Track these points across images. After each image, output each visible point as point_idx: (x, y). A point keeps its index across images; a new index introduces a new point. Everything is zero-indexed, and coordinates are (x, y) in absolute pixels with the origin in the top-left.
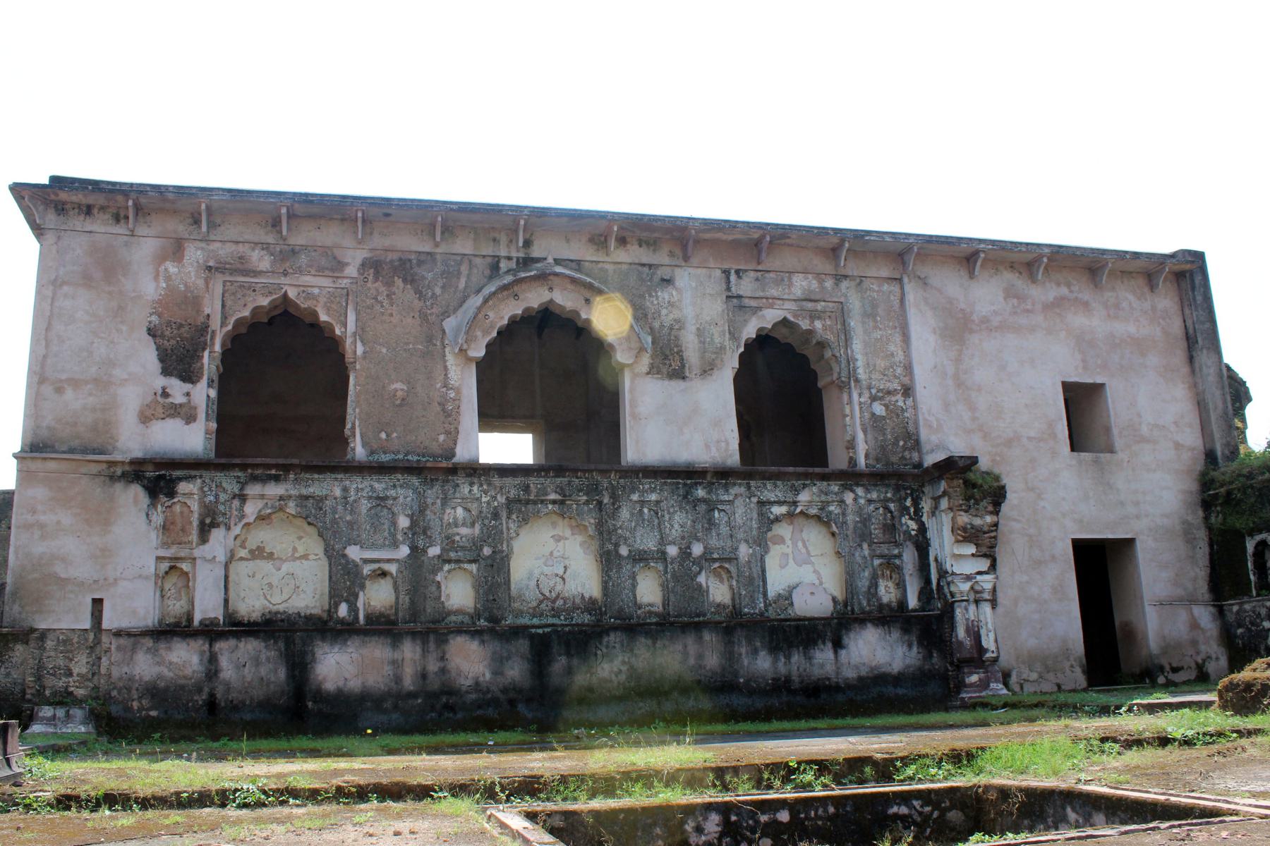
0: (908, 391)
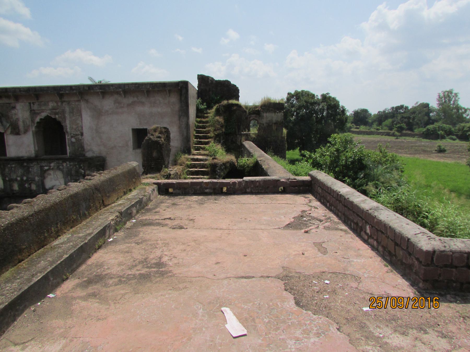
0: (82, 134)
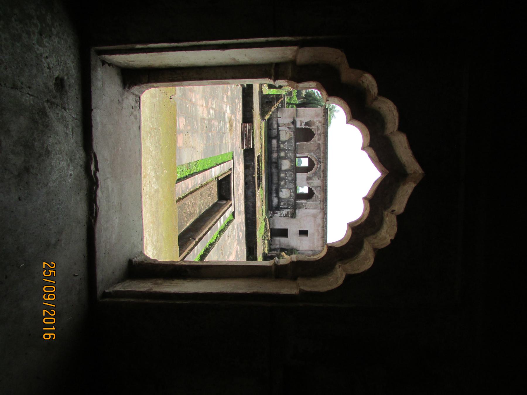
0: (306, 208)
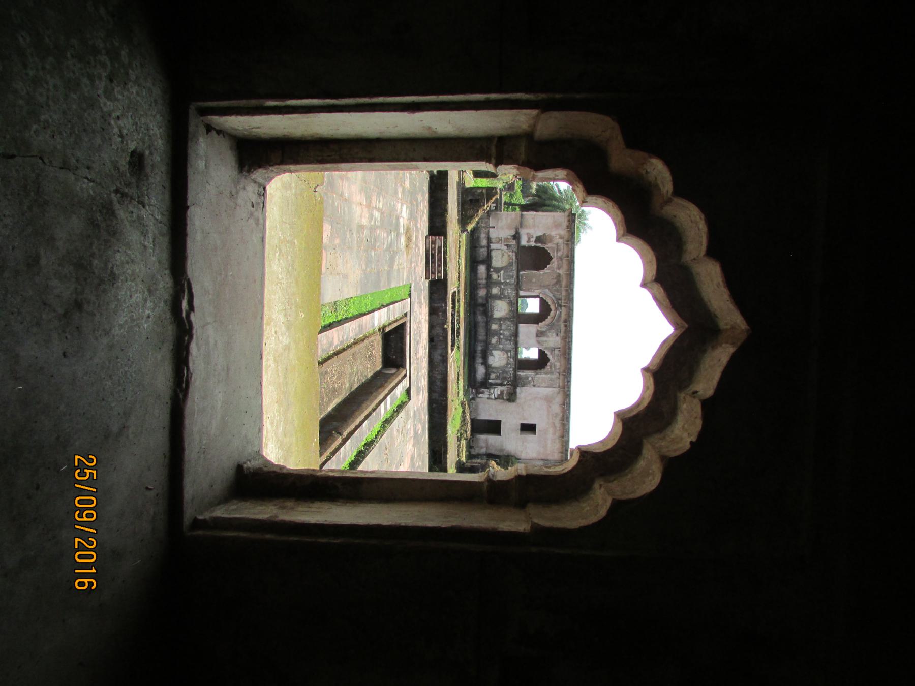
0: (534, 386)
